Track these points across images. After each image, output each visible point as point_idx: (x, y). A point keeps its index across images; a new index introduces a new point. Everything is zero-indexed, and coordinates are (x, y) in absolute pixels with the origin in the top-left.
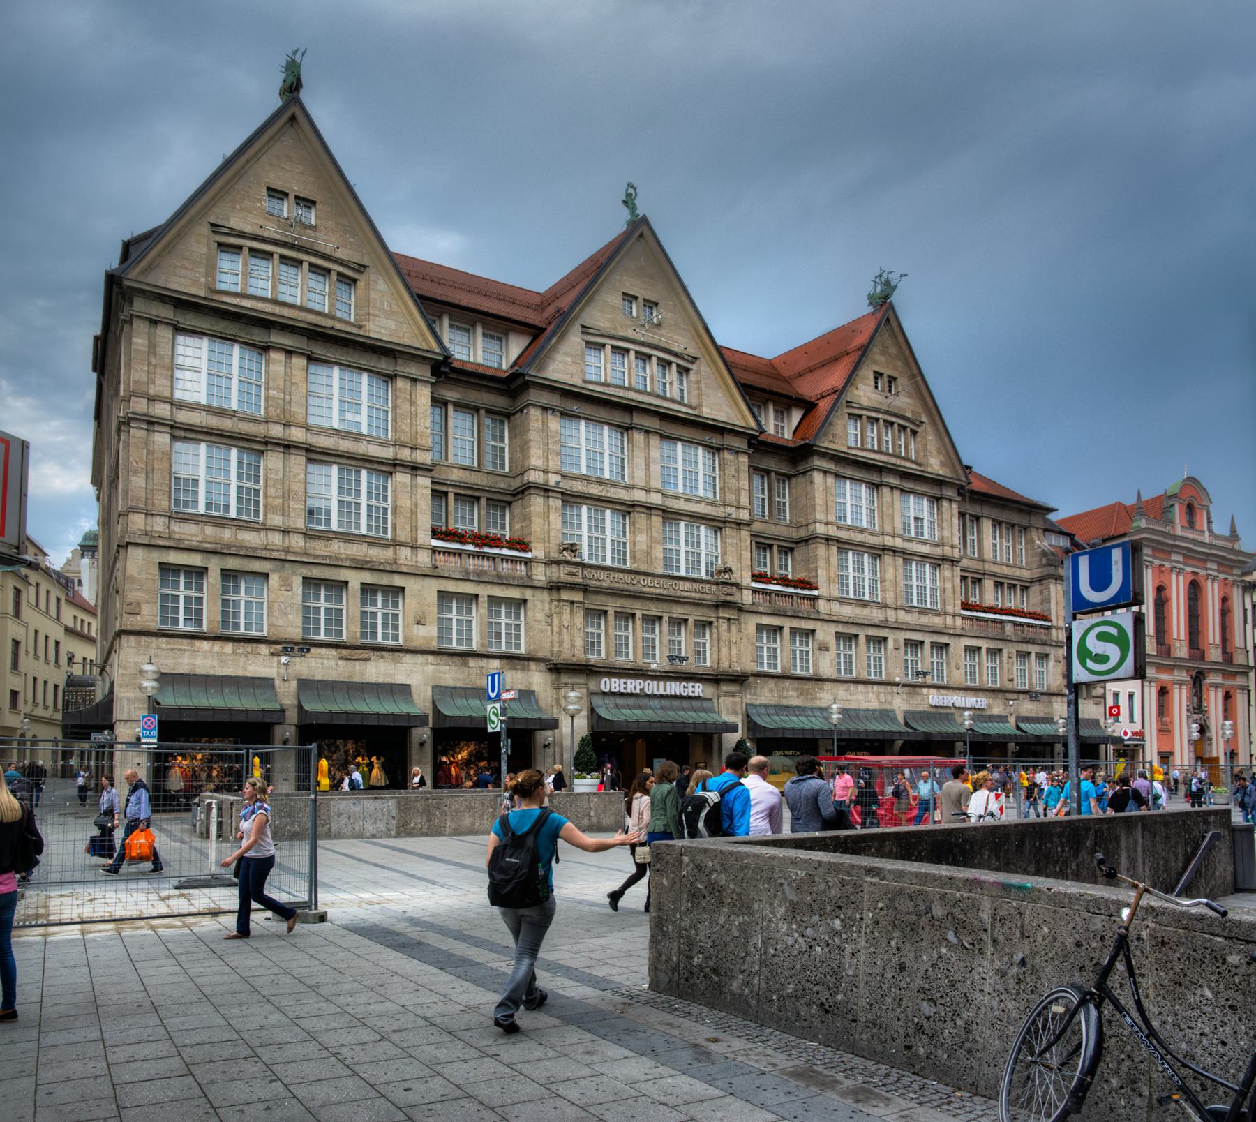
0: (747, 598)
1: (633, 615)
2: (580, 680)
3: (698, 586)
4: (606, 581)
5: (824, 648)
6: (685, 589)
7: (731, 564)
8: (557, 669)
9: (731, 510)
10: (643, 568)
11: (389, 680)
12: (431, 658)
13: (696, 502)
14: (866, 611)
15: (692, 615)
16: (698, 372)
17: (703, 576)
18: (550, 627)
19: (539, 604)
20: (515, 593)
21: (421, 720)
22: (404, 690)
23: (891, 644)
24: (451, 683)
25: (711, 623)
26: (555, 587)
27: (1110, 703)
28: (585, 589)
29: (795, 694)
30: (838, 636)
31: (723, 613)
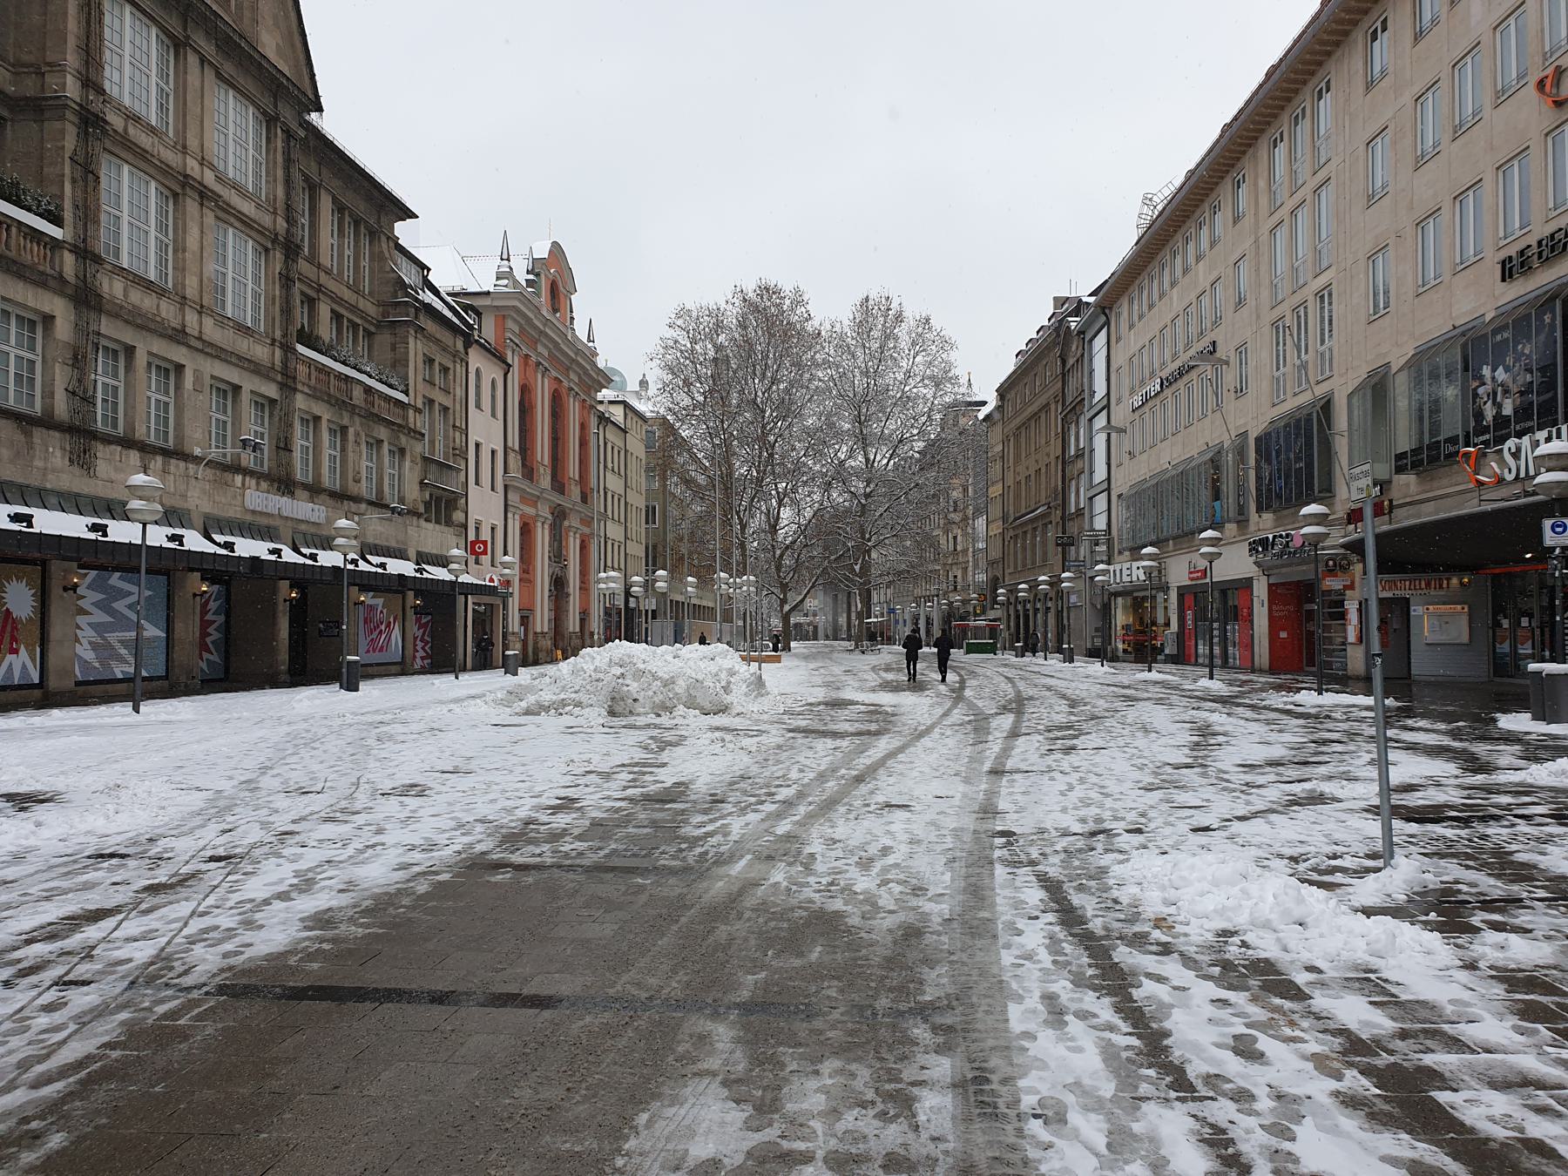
27: (472, 536)
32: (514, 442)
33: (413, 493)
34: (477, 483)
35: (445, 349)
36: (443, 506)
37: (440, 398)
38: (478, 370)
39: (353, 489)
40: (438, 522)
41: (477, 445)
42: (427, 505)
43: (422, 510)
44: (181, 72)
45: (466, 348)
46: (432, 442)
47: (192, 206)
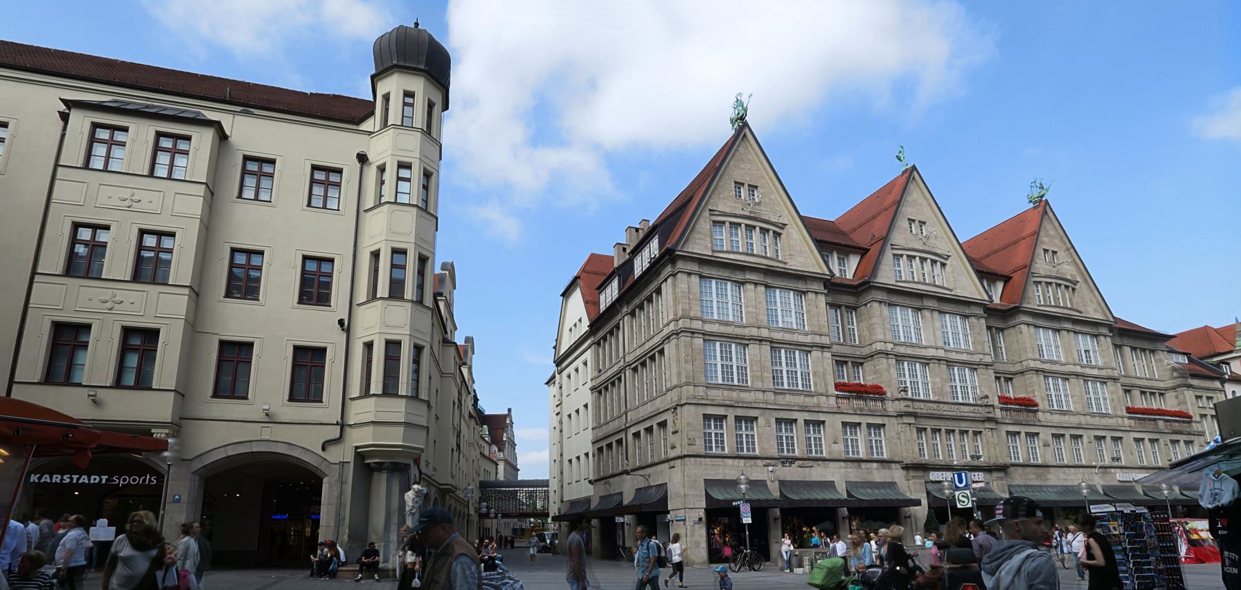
0: (998, 414)
1: (939, 430)
2: (920, 473)
3: (972, 408)
5: (1046, 445)
8: (907, 468)
14: (1067, 418)
15: (971, 427)
18: (899, 441)
19: (893, 425)
23: (1085, 439)
25: (980, 432)
26: (900, 415)
28: (915, 415)
30: (1053, 435)
31: (988, 425)
35: (1208, 389)
45: (1222, 385)
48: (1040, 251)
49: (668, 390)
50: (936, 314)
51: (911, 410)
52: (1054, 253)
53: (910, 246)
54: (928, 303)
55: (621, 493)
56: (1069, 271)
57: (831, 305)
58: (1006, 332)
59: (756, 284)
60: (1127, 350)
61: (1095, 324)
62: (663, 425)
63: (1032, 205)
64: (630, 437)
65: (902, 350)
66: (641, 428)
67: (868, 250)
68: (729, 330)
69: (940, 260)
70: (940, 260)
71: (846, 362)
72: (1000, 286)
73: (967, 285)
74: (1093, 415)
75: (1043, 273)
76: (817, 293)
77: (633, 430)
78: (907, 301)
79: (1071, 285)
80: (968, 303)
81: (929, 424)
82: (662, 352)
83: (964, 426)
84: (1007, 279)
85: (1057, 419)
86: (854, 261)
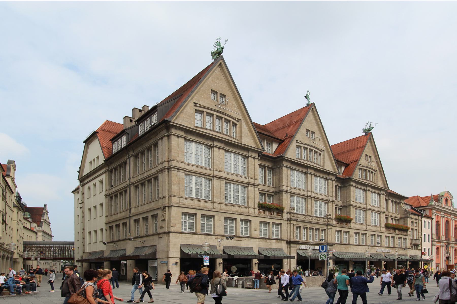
3: (323, 219)
4: (301, 218)
6: (320, 221)
7: (330, 213)
9: (330, 198)
10: (309, 214)
11: (247, 246)
12: (258, 240)
13: (322, 195)
15: (321, 227)
16: (324, 155)
17: (323, 217)
20: (278, 222)
21: (255, 257)
22: (251, 248)
24: (263, 247)
25: (325, 230)
27: (423, 251)
29: (344, 249)
32: (434, 231)
33: (409, 245)
34: (424, 241)
36: (416, 246)
37: (414, 228)
38: (425, 221)
39: (396, 246)
40: (415, 249)
41: (424, 234)
42: (412, 247)
43: (411, 248)
44: (366, 194)
46: (413, 236)
47: (368, 212)
48: (364, 155)
49: (160, 198)
50: (313, 176)
51: (295, 218)
52: (370, 157)
53: (306, 142)
54: (310, 171)
55: (125, 249)
56: (374, 165)
57: (260, 165)
58: (342, 189)
59: (219, 149)
60: (390, 201)
61: (380, 189)
62: (155, 217)
63: (364, 134)
64: (132, 222)
65: (294, 191)
66: (140, 217)
67: (283, 141)
68: (201, 170)
69: (318, 152)
70: (318, 152)
71: (265, 194)
72: (343, 168)
73: (329, 166)
74: (372, 226)
75: (363, 165)
76: (254, 158)
77: (135, 218)
78: (300, 169)
79: (373, 172)
80: (328, 173)
81: (302, 225)
82: (156, 178)
83: (318, 226)
84: (347, 165)
85: (356, 226)
86: (275, 146)
